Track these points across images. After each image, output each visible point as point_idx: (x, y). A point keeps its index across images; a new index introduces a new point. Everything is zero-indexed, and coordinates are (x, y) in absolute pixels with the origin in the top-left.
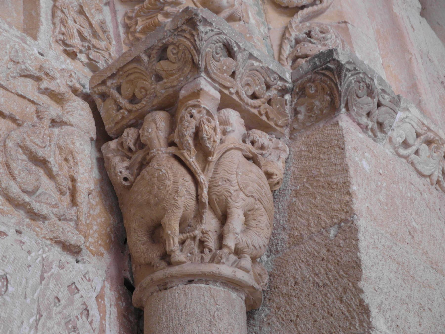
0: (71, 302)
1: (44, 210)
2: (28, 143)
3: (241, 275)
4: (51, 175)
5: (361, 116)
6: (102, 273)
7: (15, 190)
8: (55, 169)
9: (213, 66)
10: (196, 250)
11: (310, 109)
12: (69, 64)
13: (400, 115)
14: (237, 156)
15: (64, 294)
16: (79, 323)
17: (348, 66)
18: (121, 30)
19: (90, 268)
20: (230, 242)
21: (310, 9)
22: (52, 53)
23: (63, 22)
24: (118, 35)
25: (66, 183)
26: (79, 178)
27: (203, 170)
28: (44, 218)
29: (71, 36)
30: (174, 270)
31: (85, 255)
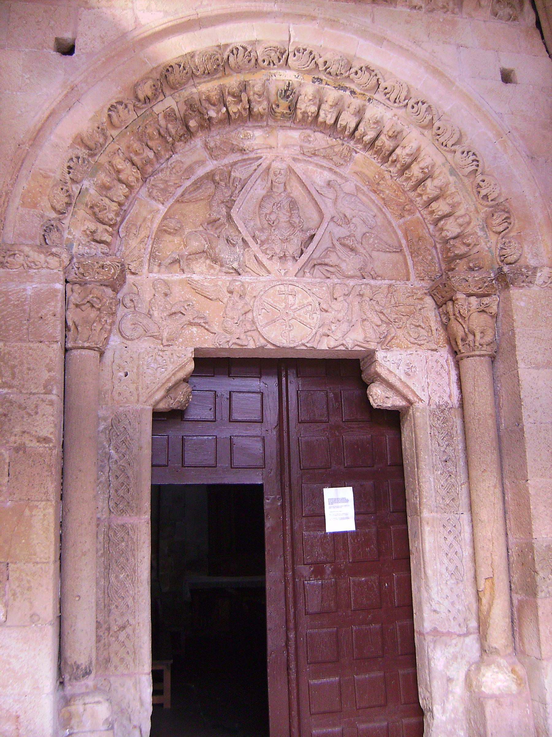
0: (437, 366)
1: (422, 342)
2: (413, 323)
3: (482, 353)
4: (422, 328)
5: (519, 284)
6: (446, 352)
7: (412, 340)
8: (424, 327)
9: (460, 288)
10: (468, 347)
11: (502, 286)
12: (423, 283)
13: (539, 274)
14: (475, 315)
15: (434, 364)
16: (441, 372)
17: (508, 272)
18: (440, 255)
19: (442, 353)
20: (477, 344)
21: (504, 232)
22: (416, 282)
23: (417, 269)
24: (439, 258)
25: (427, 328)
26: (432, 325)
27: (465, 323)
28: (423, 344)
29: (421, 273)
30: (462, 355)
31: (439, 349)
